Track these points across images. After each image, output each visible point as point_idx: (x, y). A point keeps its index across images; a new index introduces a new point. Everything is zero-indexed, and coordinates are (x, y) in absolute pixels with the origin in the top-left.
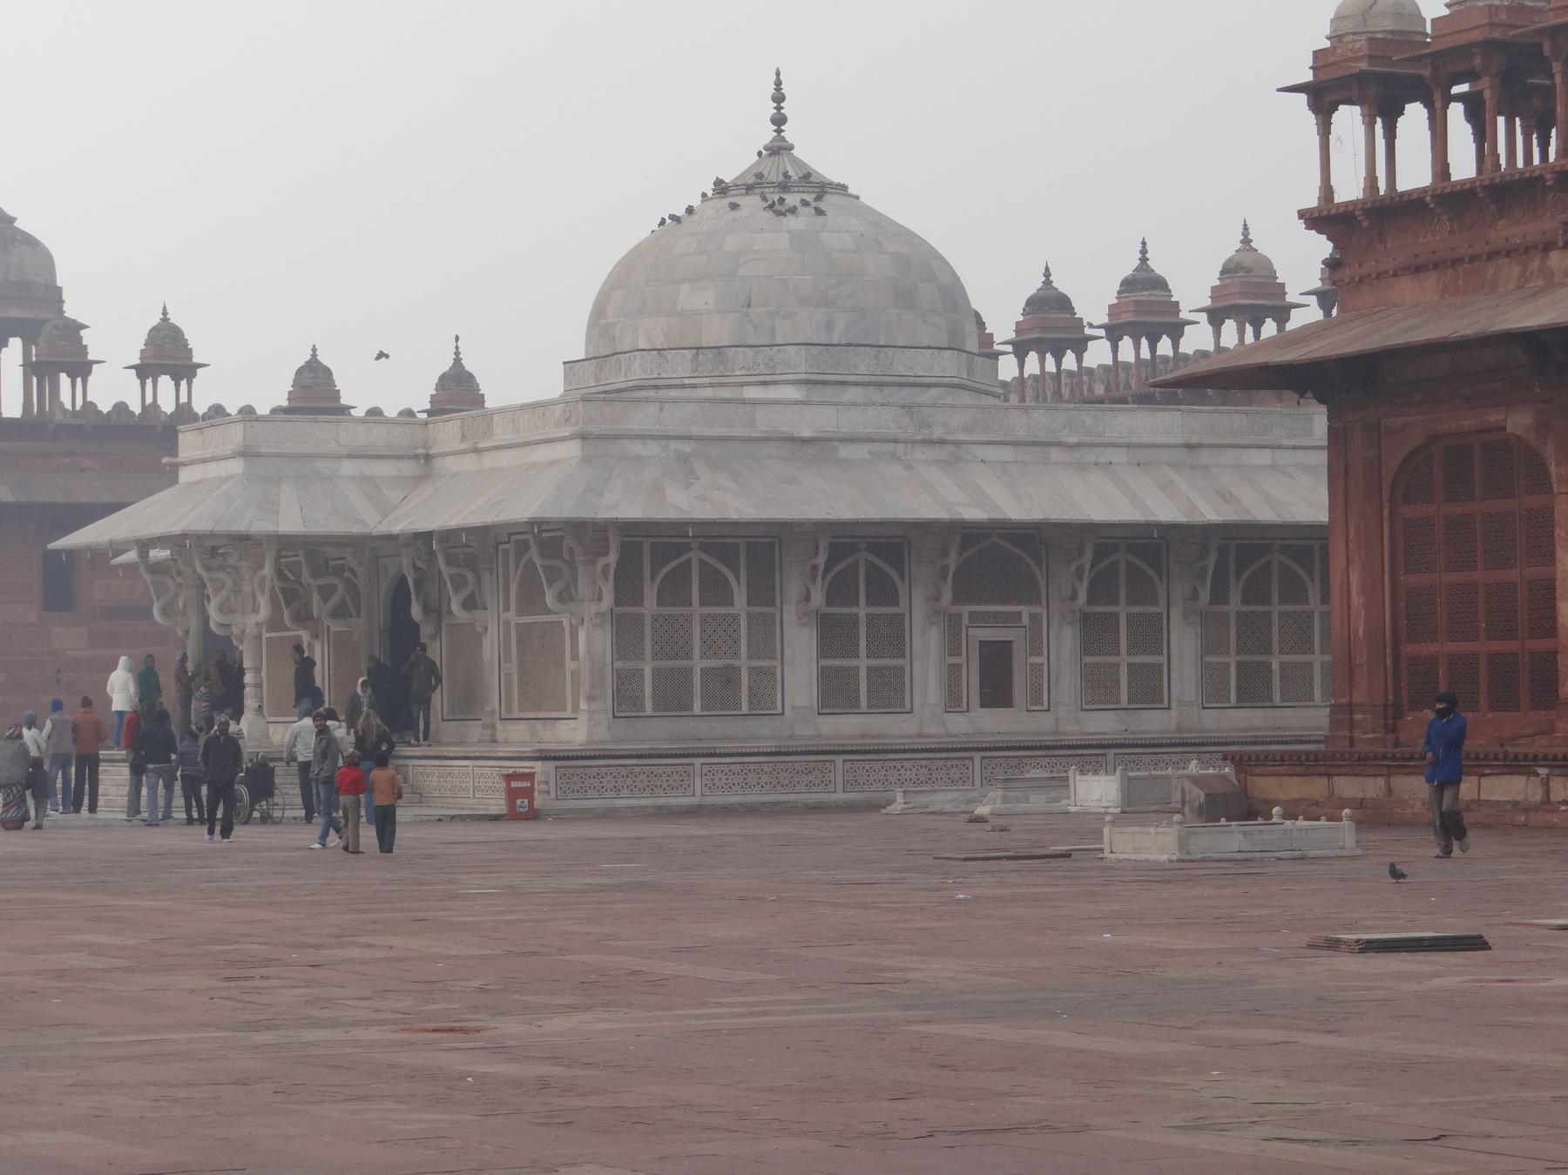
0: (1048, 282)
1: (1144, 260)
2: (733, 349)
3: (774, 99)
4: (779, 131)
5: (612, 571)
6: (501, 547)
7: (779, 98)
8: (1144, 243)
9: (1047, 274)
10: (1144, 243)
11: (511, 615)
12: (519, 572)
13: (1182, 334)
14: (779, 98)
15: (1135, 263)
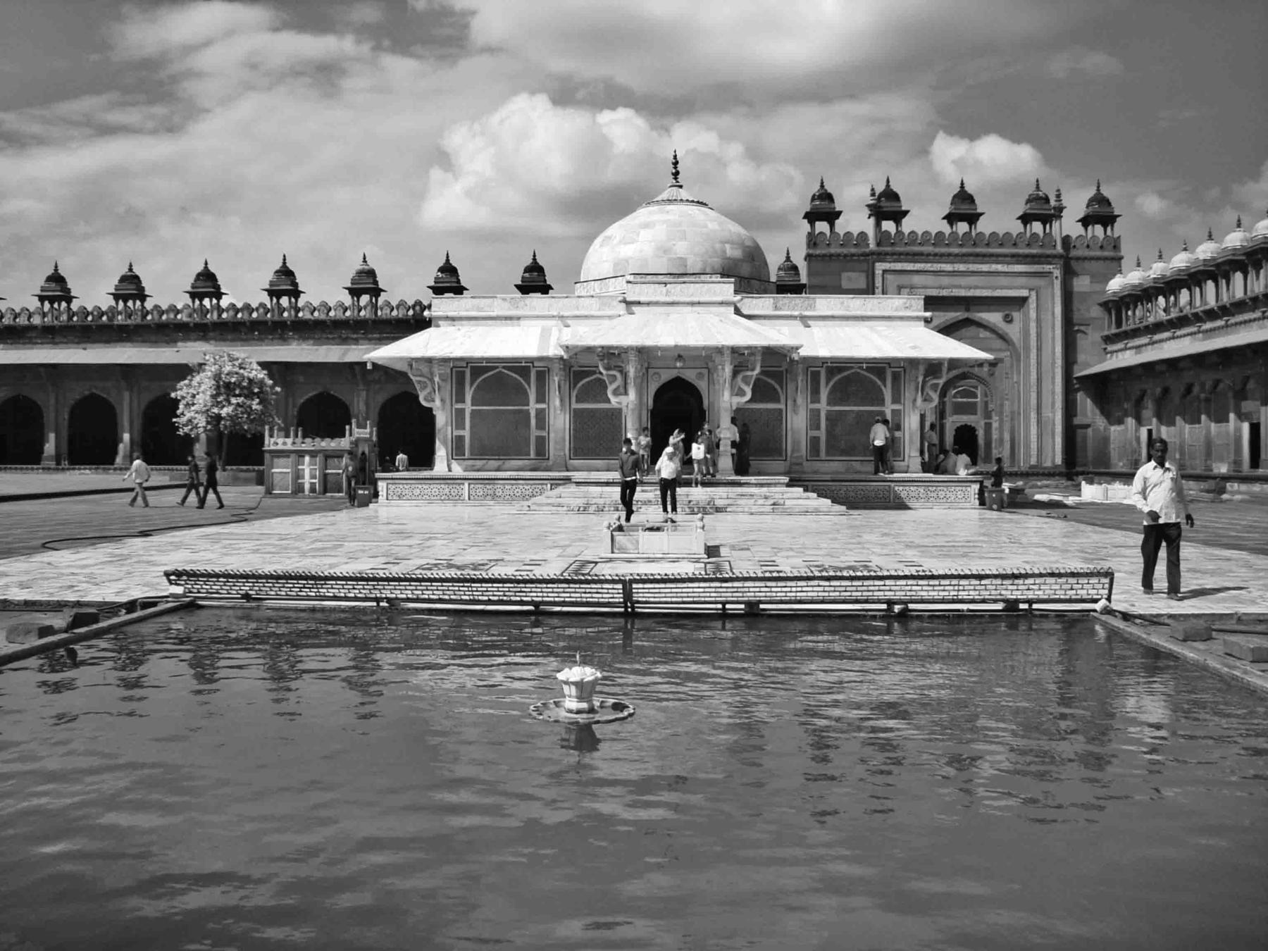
0: (206, 267)
1: (284, 263)
2: (753, 281)
3: (673, 164)
4: (676, 179)
5: (940, 387)
6: (810, 369)
7: (676, 163)
8: (284, 256)
9: (206, 263)
10: (284, 256)
11: (823, 406)
12: (831, 383)
13: (299, 296)
14: (676, 163)
15: (281, 264)
